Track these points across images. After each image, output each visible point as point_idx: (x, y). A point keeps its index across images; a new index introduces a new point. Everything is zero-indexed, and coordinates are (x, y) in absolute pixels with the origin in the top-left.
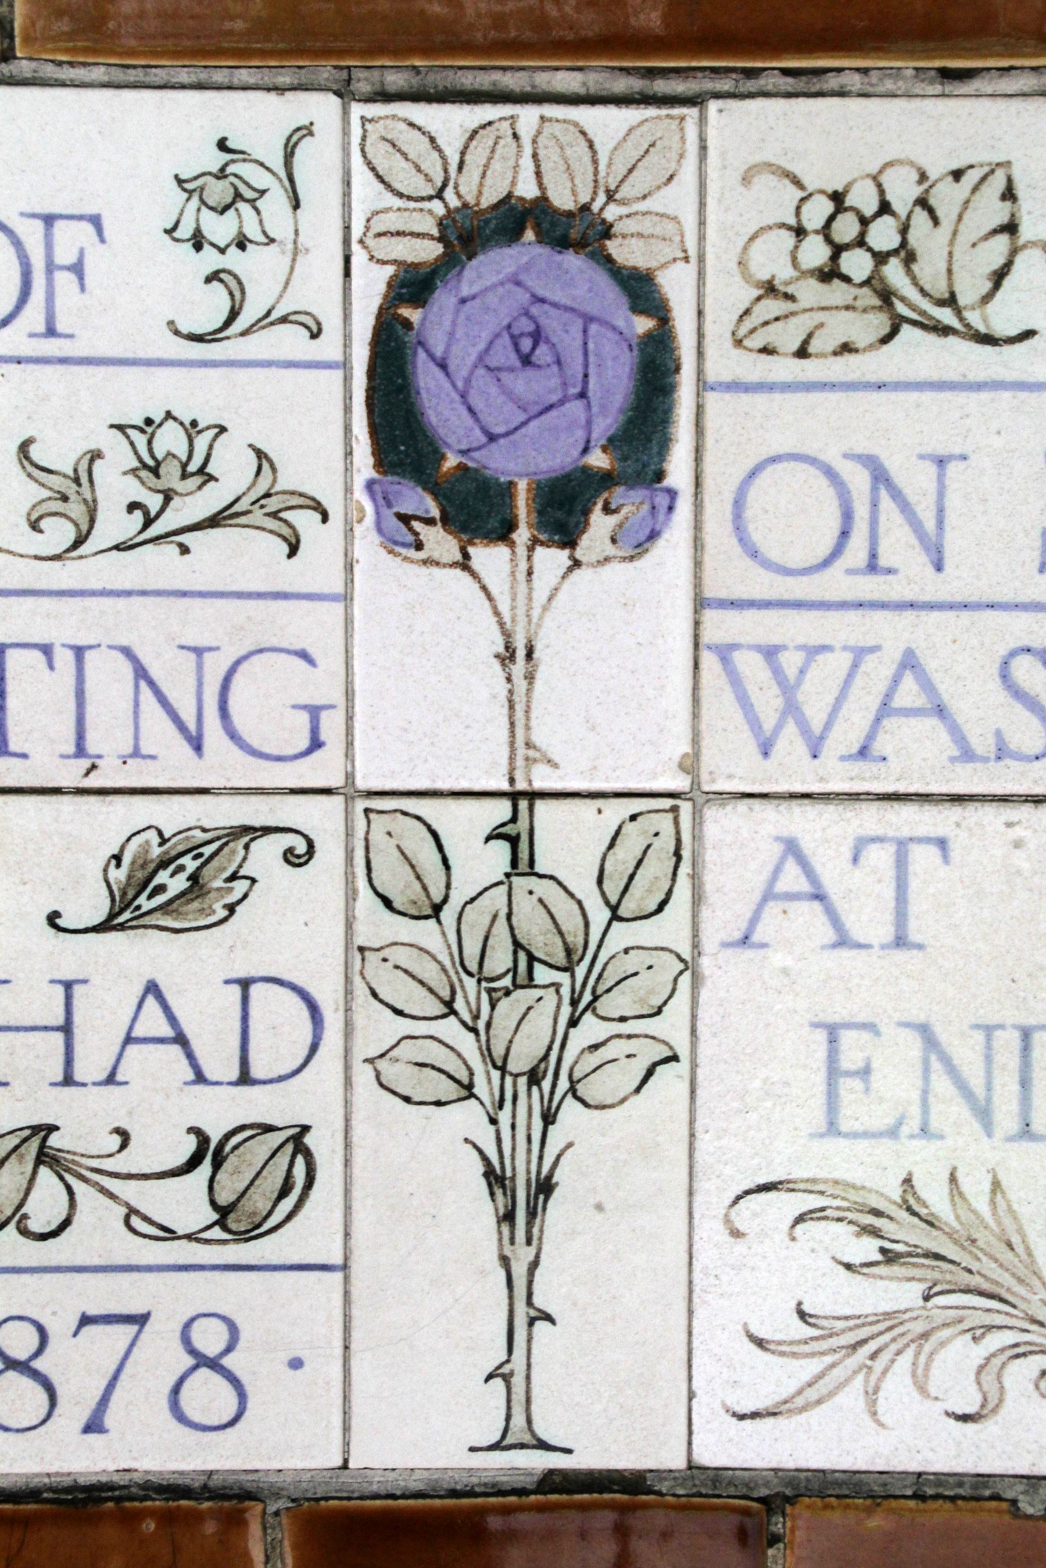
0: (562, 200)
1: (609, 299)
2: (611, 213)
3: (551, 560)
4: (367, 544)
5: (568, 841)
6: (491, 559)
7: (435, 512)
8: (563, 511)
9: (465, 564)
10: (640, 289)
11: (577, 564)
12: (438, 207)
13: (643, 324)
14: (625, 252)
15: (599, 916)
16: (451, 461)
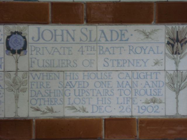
0: (19, 31)
1: (22, 38)
2: (22, 32)
3: (18, 55)
4: (6, 55)
5: (20, 74)
6: (15, 55)
7: (10, 52)
8: (19, 52)
9: (12, 56)
10: (24, 38)
11: (20, 56)
12: (10, 32)
13: (25, 40)
14: (23, 35)
15: (22, 79)
16: (11, 49)
